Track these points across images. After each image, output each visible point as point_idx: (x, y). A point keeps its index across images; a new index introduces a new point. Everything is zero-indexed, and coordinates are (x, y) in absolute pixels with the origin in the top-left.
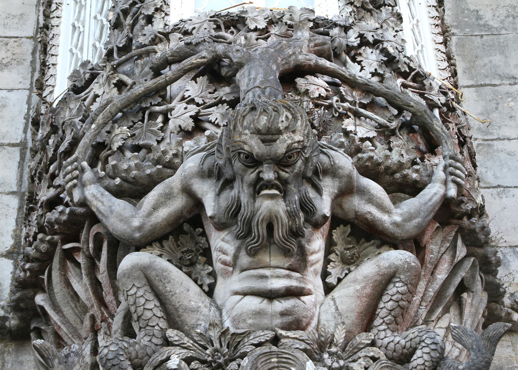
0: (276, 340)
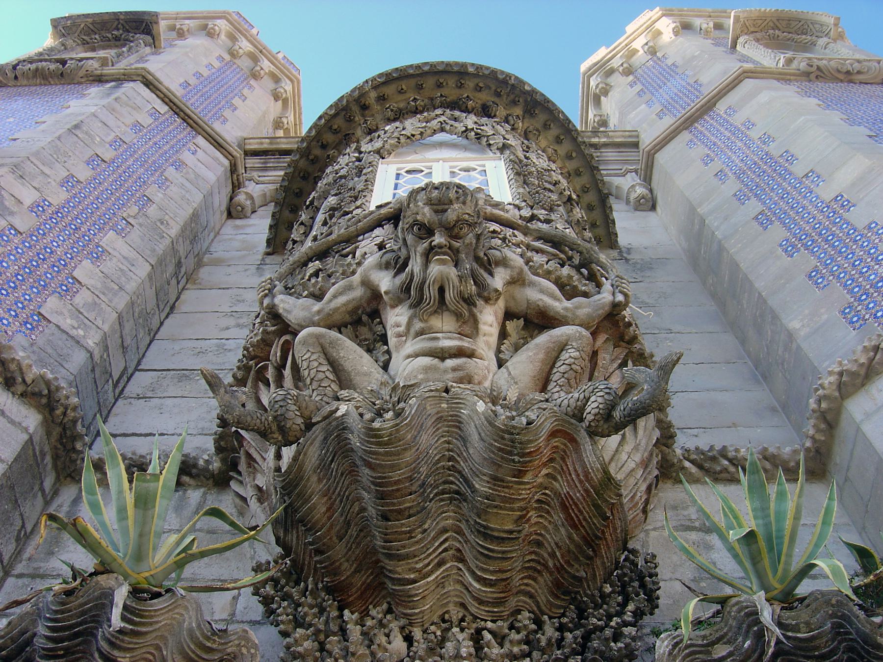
0: (447, 391)
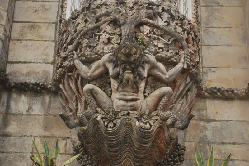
0: (128, 114)
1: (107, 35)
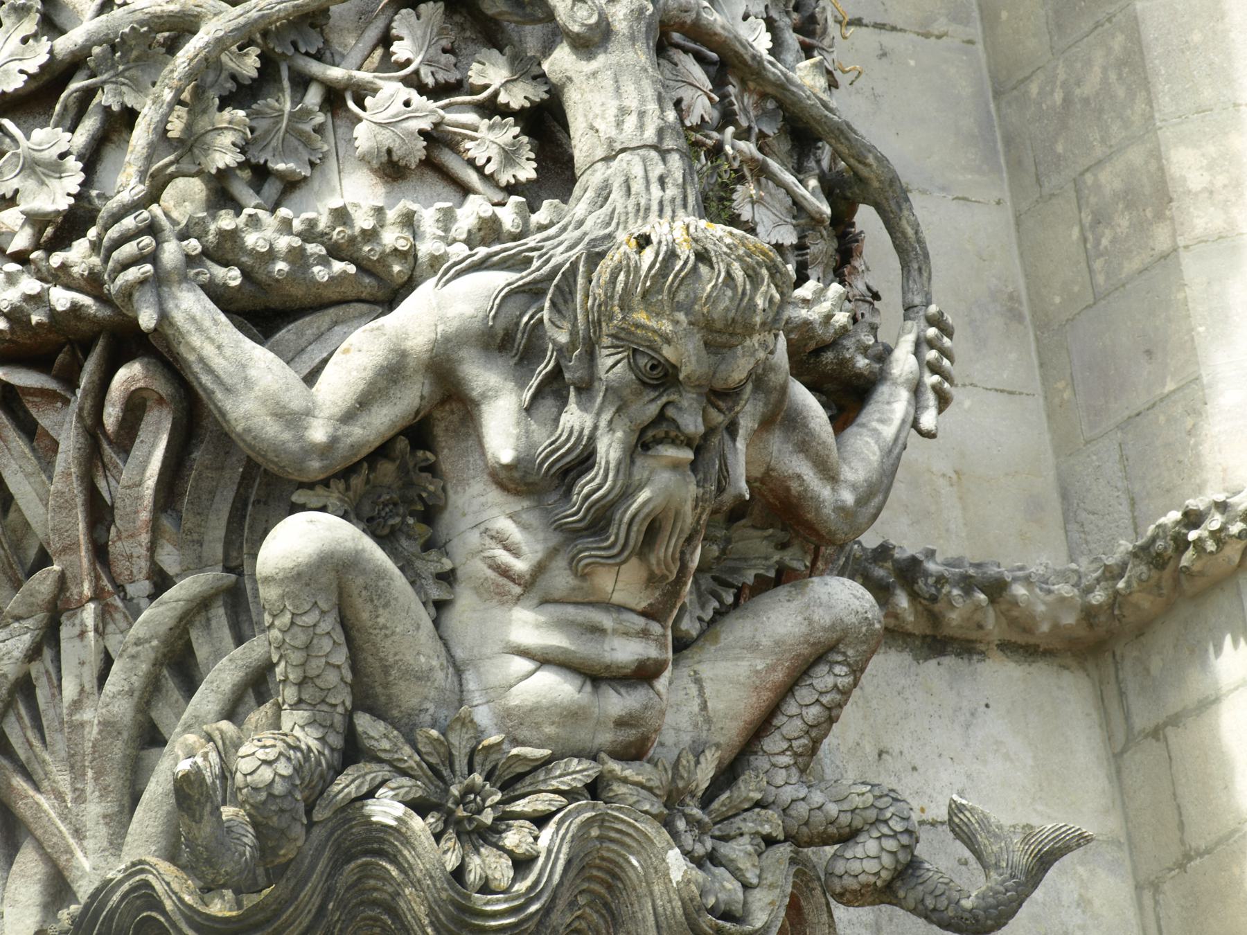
1: (412, 94)
